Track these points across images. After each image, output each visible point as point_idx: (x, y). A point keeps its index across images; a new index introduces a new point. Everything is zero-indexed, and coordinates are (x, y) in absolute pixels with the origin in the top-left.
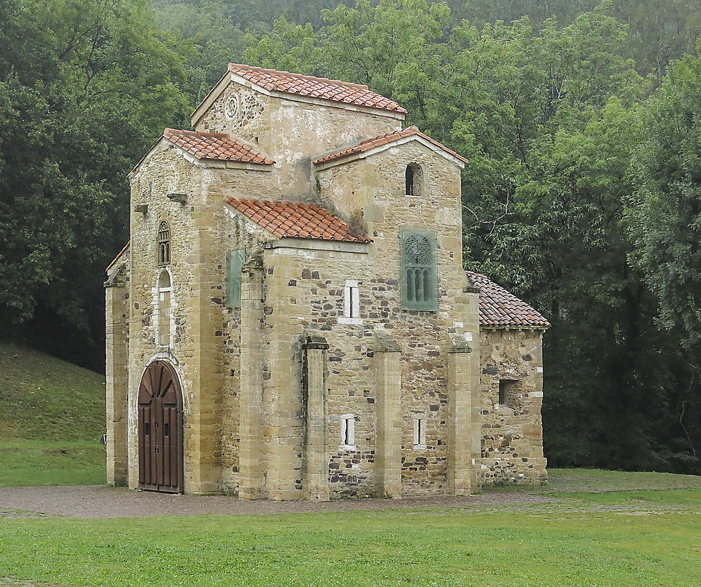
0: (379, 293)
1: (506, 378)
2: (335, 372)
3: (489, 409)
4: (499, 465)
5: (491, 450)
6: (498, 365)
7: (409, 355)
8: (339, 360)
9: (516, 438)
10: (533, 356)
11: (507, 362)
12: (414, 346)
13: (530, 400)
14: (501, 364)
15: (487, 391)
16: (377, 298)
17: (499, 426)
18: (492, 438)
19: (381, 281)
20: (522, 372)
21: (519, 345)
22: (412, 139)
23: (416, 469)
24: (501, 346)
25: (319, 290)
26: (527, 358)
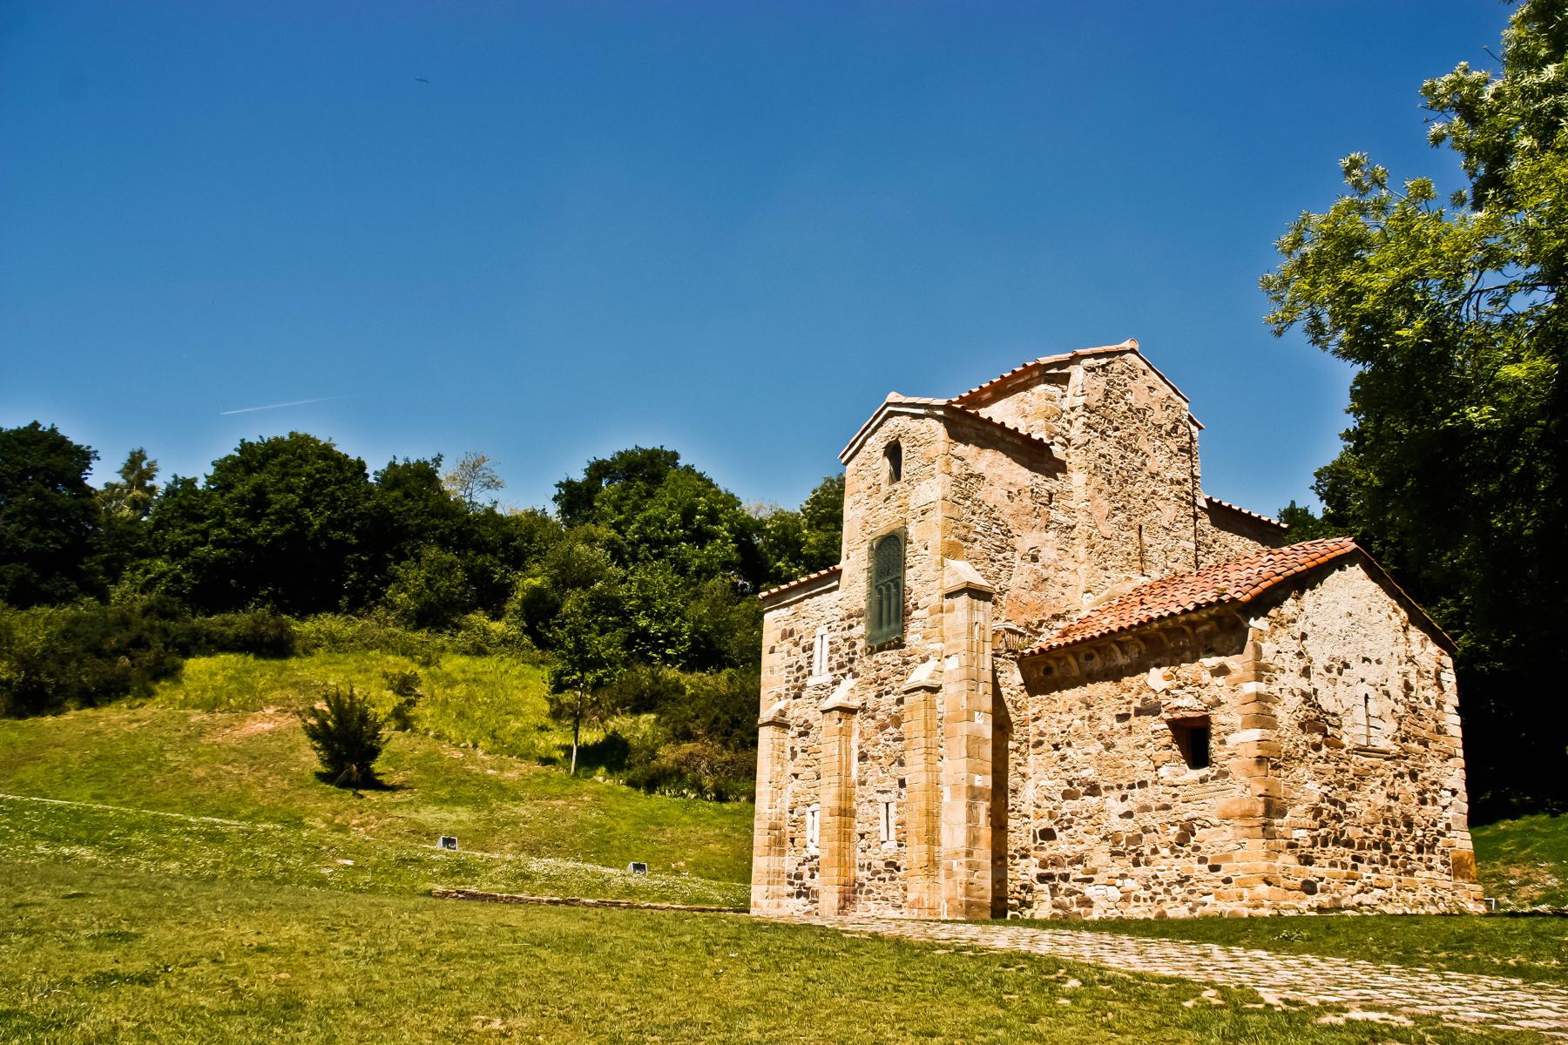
0: (846, 634)
1: (1177, 715)
2: (803, 751)
4: (1160, 880)
6: (1162, 696)
7: (874, 710)
8: (806, 734)
12: (879, 696)
15: (1143, 746)
16: (845, 640)
17: (1166, 807)
18: (1155, 831)
19: (850, 616)
22: (885, 412)
23: (884, 880)
25: (795, 650)
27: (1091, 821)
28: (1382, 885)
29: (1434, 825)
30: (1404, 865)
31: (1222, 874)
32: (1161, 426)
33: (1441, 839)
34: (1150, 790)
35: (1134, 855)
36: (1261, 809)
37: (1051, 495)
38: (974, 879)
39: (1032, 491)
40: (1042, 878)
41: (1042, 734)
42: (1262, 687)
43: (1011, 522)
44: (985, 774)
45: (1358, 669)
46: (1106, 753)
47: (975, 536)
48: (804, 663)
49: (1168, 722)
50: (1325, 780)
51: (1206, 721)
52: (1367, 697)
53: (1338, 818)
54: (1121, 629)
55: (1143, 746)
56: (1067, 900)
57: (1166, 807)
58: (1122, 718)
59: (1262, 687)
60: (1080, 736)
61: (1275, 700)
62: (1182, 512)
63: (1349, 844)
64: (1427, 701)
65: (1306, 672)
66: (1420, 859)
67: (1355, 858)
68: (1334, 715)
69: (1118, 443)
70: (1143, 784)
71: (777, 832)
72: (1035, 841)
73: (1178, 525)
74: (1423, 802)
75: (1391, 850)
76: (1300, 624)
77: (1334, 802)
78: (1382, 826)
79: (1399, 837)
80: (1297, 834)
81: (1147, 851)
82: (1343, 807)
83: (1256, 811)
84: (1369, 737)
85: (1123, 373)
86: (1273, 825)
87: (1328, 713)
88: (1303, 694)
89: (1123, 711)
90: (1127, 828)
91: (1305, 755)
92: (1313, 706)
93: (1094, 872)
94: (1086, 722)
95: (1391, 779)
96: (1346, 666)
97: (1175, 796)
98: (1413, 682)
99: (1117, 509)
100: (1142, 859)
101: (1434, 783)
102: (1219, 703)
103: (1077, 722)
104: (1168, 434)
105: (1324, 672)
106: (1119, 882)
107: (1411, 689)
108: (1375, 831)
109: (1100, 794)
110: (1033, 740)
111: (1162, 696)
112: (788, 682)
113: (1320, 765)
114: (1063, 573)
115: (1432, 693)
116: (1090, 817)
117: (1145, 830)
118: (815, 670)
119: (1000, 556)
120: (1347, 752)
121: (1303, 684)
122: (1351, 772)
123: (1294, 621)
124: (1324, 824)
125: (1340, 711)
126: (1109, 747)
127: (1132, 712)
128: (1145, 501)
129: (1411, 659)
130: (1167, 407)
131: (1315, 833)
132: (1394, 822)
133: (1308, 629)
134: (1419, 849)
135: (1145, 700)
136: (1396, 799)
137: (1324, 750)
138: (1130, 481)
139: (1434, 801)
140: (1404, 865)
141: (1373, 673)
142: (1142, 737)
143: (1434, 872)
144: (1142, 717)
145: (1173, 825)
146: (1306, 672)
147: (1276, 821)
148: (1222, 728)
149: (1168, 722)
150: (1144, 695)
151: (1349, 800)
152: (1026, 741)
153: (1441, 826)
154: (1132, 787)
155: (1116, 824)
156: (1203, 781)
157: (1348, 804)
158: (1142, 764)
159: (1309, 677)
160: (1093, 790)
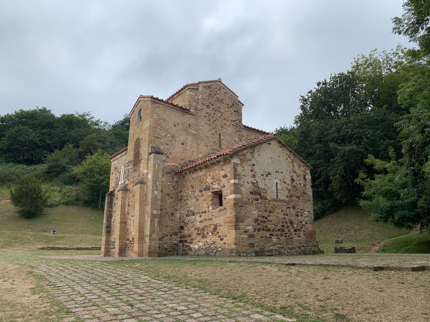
1: (214, 191)
3: (206, 210)
5: (208, 233)
6: (210, 184)
7: (132, 191)
9: (220, 226)
10: (228, 174)
11: (215, 182)
13: (227, 201)
14: (212, 183)
15: (205, 200)
17: (211, 219)
18: (208, 227)
20: (222, 185)
21: (220, 170)
24: (211, 173)
26: (225, 176)
27: (193, 224)
28: (281, 243)
29: (301, 222)
30: (289, 236)
31: (224, 241)
32: (228, 104)
33: (304, 227)
34: (207, 214)
35: (202, 234)
36: (234, 220)
37: (190, 125)
38: (152, 244)
39: (183, 124)
40: (181, 241)
41: (182, 196)
42: (237, 181)
43: (174, 133)
44: (158, 210)
45: (274, 175)
46: (196, 202)
47: (161, 137)
48: (118, 177)
49: (212, 192)
50: (260, 210)
51: (221, 191)
52: (277, 183)
53: (264, 222)
54: (199, 164)
55: (205, 200)
56: (186, 249)
57: (211, 219)
58: (201, 191)
59: (237, 181)
60: (190, 197)
61: (241, 185)
62: (234, 130)
63: (269, 230)
64: (300, 184)
65: (254, 176)
66: (295, 234)
67: (270, 235)
68: (264, 189)
69: (213, 109)
70: (205, 212)
71: (109, 229)
72: (179, 230)
73: (233, 134)
74: (298, 216)
75: (284, 231)
76: (252, 161)
77: (263, 217)
78: (281, 224)
79: (288, 227)
80: (248, 228)
81: (206, 234)
82: (266, 218)
83: (233, 221)
84: (277, 195)
85: (216, 88)
86: (239, 225)
87: (261, 189)
88: (252, 183)
89: (201, 189)
90: (201, 226)
91: (252, 202)
92: (256, 186)
93: (193, 240)
94: (192, 193)
95: (286, 209)
96: (269, 174)
97: (213, 216)
98: (295, 178)
99: (212, 129)
100: (204, 236)
101: (302, 210)
102: (224, 186)
103: (190, 193)
104: (231, 106)
105: (261, 176)
106: (198, 243)
107: (294, 181)
108: (279, 225)
109: (195, 215)
110: (180, 198)
111: (210, 184)
112: (115, 183)
113: (259, 205)
114: (193, 148)
115: (302, 182)
116: (192, 222)
117: (205, 226)
118: (121, 180)
119: (170, 143)
120: (269, 201)
121: (253, 180)
122: (270, 207)
123: (250, 160)
124: (258, 224)
125: (266, 188)
126: (197, 200)
127: (203, 189)
128: (222, 126)
129: (294, 172)
130: (231, 99)
131: (256, 227)
132: (286, 222)
133: (255, 163)
134: (295, 230)
135: (206, 186)
136: (287, 215)
137: (260, 201)
138: (216, 120)
139: (301, 215)
140: (289, 236)
141: (280, 176)
142: (205, 197)
143: (301, 238)
144: (205, 191)
145: (212, 225)
146: (254, 176)
147: (240, 224)
148: (225, 194)
149: (212, 192)
150: (206, 184)
151: (269, 216)
152: (177, 199)
153: (304, 223)
154: (202, 213)
155: (198, 225)
156: (220, 211)
157: (268, 218)
158: (205, 205)
159: (255, 178)
160: (193, 214)
